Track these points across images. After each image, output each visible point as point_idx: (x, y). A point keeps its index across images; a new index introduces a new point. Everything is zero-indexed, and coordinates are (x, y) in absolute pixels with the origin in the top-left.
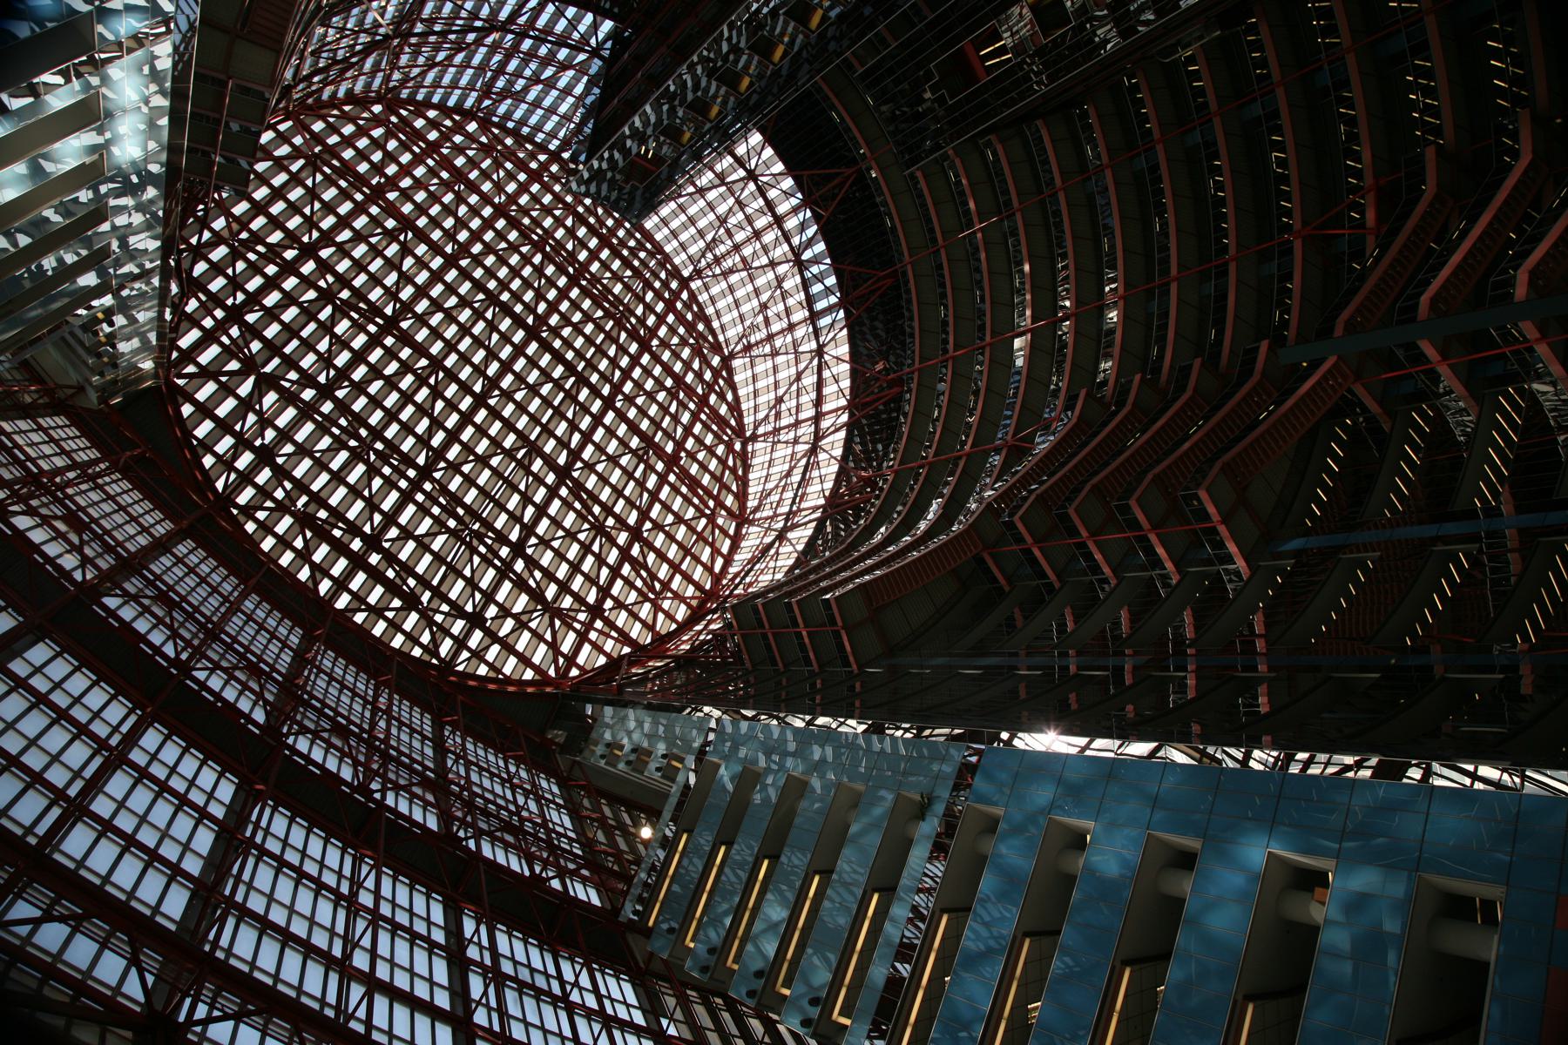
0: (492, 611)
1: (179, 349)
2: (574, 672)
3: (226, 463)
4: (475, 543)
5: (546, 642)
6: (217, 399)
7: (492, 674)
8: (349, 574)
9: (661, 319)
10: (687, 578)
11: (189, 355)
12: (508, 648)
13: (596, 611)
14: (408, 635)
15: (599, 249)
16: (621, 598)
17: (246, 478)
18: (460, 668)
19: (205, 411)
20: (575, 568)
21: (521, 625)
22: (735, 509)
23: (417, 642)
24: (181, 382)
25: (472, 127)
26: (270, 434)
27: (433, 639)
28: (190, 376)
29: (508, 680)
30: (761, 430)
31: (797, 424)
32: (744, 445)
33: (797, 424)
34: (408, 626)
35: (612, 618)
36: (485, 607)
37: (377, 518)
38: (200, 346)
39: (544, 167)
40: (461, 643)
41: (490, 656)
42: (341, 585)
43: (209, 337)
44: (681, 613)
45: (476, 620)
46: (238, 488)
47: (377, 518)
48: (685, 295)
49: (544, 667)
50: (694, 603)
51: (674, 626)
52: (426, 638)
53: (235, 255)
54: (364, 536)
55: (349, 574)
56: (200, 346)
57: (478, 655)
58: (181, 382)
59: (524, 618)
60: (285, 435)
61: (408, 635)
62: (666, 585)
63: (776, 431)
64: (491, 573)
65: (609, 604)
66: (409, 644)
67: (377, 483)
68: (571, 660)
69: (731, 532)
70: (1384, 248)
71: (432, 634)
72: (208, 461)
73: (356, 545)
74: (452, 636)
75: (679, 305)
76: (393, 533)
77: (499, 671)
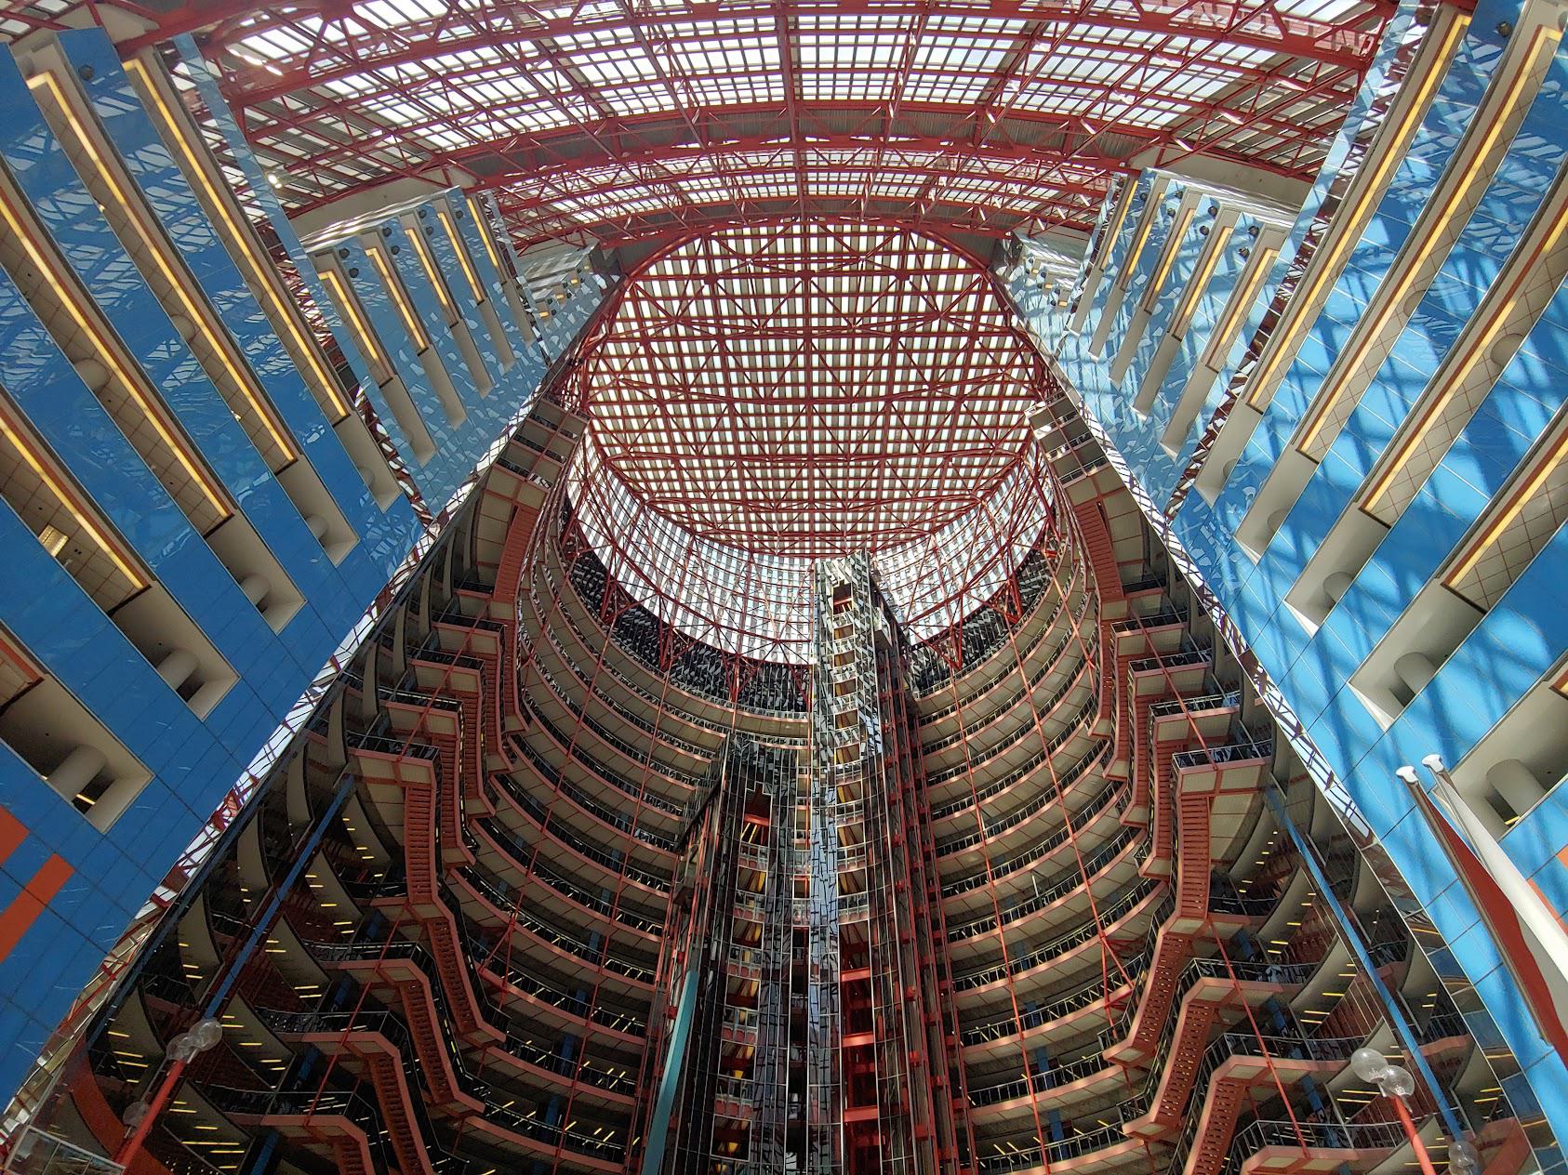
0: (706, 291)
1: (989, 293)
4: (748, 323)
5: (659, 298)
6: (950, 283)
7: (675, 253)
9: (748, 522)
10: (608, 403)
11: (981, 294)
12: (678, 277)
13: (645, 341)
15: (812, 527)
18: (697, 242)
19: (952, 271)
20: (679, 355)
21: (683, 297)
22: (616, 463)
23: (735, 237)
24: (976, 276)
25: (927, 527)
26: (908, 287)
27: (726, 247)
28: (973, 285)
29: (662, 258)
30: (642, 516)
31: (629, 540)
32: (643, 501)
33: (629, 540)
34: (748, 243)
36: (712, 290)
37: (814, 290)
38: (980, 303)
39: (874, 541)
40: (709, 257)
43: (978, 311)
45: (711, 278)
47: (814, 290)
48: (746, 544)
52: (732, 244)
53: (996, 365)
54: (813, 274)
56: (980, 303)
58: (976, 276)
60: (900, 294)
62: (618, 389)
63: (634, 525)
64: (725, 312)
65: (642, 351)
67: (830, 309)
68: (636, 300)
69: (606, 449)
70: (472, 973)
71: (731, 250)
72: (931, 245)
74: (717, 257)
75: (744, 537)
77: (673, 259)
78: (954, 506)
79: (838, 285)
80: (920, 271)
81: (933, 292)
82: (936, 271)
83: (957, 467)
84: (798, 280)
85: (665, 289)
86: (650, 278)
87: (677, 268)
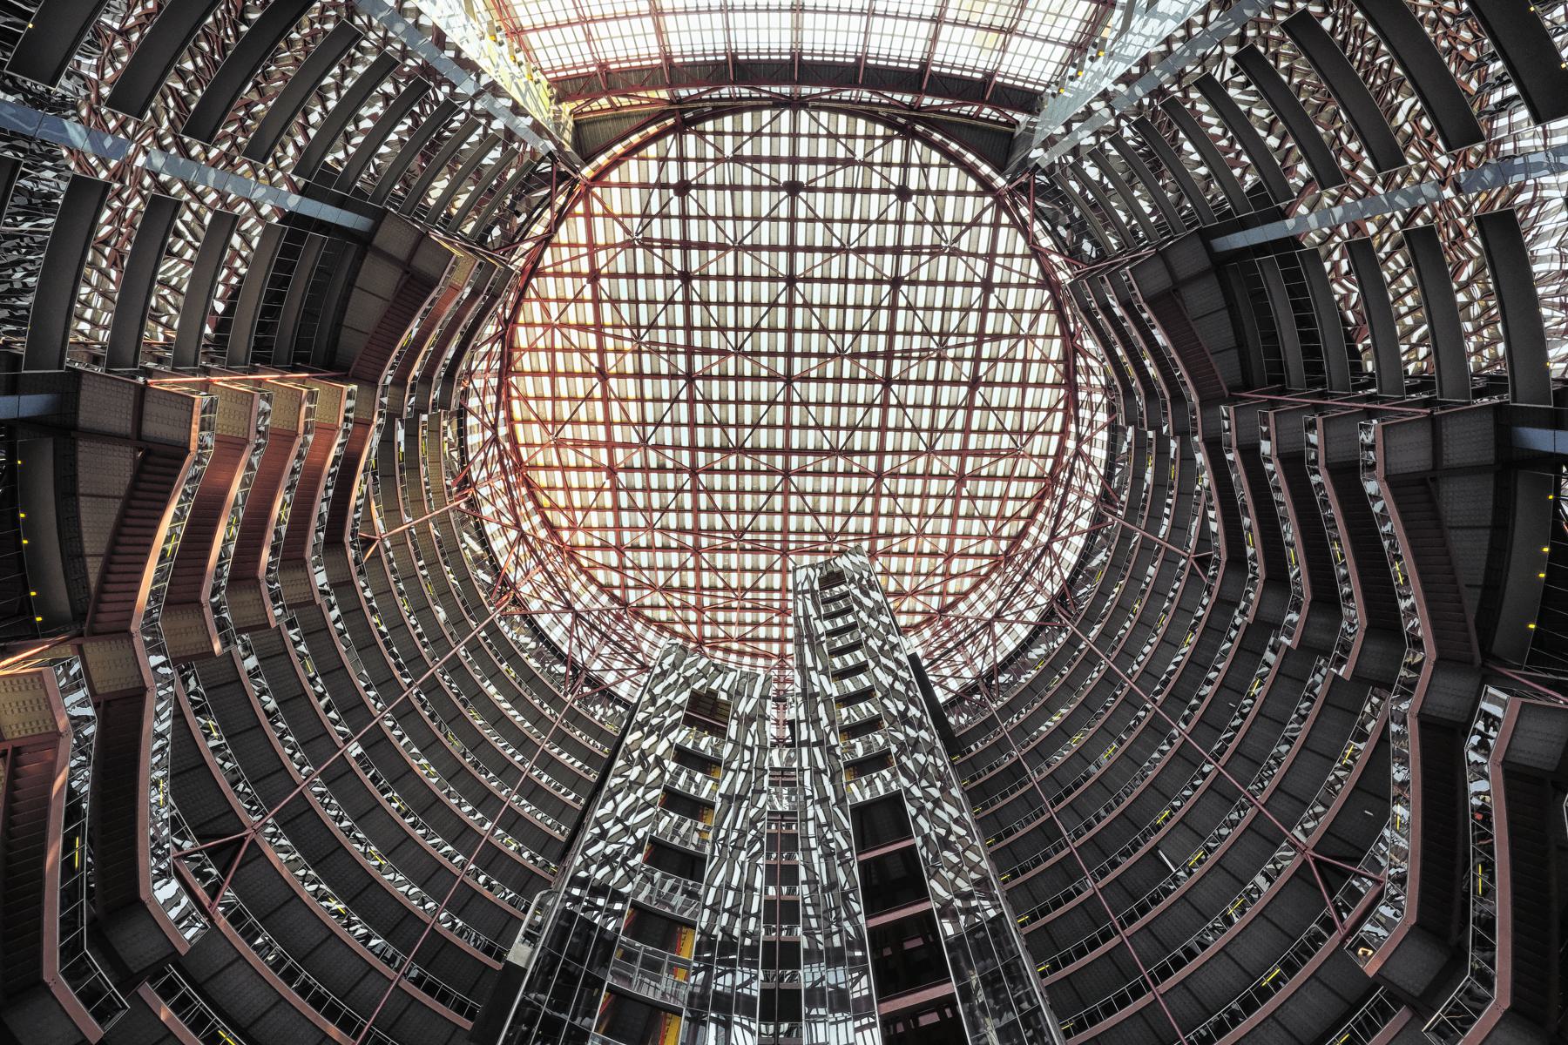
0: (674, 208)
3: (924, 166)
7: (642, 153)
8: (794, 147)
11: (996, 225)
14: (722, 133)
16: (580, 305)
17: (905, 165)
19: (961, 193)
23: (715, 133)
24: (989, 200)
28: (984, 210)
35: (577, 280)
41: (653, 165)
42: (794, 135)
44: (522, 337)
45: (683, 188)
49: (606, 190)
50: (516, 354)
51: (521, 320)
55: (794, 147)
57: (663, 160)
59: (646, 221)
61: (722, 133)
66: (719, 128)
68: (589, 215)
69: (523, 450)
72: (936, 157)
75: (692, 616)
76: (784, 211)
78: (970, 564)
81: (938, 221)
83: (973, 498)
84: (783, 194)
86: (609, 185)
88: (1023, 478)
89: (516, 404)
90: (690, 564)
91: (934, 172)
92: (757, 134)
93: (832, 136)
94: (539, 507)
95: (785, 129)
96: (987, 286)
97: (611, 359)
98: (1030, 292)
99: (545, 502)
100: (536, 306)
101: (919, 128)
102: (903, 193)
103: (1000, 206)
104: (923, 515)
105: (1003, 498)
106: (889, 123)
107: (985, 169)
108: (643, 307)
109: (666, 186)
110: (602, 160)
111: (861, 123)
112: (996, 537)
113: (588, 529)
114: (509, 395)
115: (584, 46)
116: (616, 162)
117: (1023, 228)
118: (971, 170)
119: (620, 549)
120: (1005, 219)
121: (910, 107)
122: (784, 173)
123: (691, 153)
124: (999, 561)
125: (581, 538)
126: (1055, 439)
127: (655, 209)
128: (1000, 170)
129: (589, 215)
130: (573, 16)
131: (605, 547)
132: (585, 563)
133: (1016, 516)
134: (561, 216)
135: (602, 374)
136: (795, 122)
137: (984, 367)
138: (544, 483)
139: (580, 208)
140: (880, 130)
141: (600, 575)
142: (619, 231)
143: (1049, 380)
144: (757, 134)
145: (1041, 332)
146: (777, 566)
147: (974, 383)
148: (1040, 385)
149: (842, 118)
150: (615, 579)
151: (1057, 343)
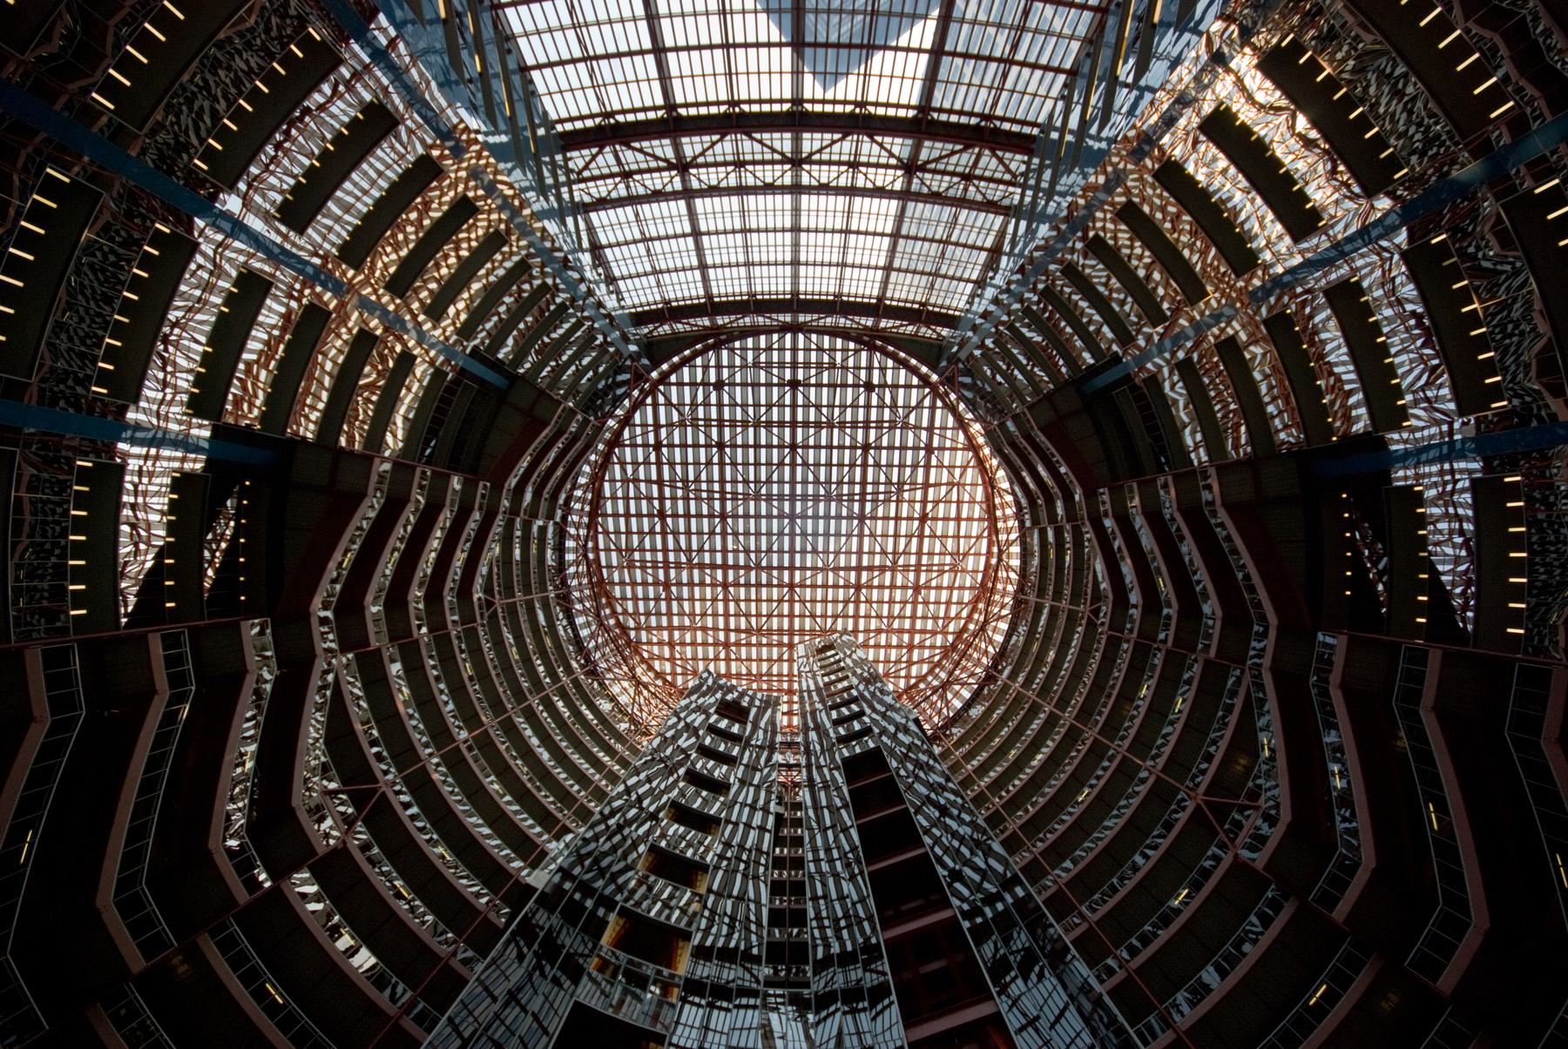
0: (713, 399)
2: (649, 400)
6: (907, 397)
11: (933, 408)
12: (693, 384)
17: (870, 368)
19: (908, 386)
40: (719, 367)
41: (699, 371)
42: (794, 350)
46: (870, 360)
68: (655, 405)
72: (890, 363)
73: (800, 375)
78: (927, 653)
79: (819, 396)
80: (883, 386)
82: (896, 386)
85: (681, 395)
86: (671, 384)
87: (693, 375)
88: (962, 588)
89: (601, 537)
90: (722, 656)
91: (889, 373)
92: (769, 349)
93: (820, 349)
94: (614, 613)
95: (788, 345)
96: (929, 449)
97: (668, 504)
98: (959, 453)
99: (619, 610)
100: (617, 467)
101: (879, 343)
102: (869, 387)
103: (935, 394)
104: (891, 617)
105: (948, 603)
106: (857, 340)
107: (924, 369)
108: (691, 468)
109: (709, 384)
110: (665, 367)
111: (839, 341)
112: (945, 633)
113: (649, 629)
114: (596, 532)
115: (655, 290)
116: (675, 368)
117: (953, 409)
118: (914, 371)
119: (671, 644)
120: (939, 403)
121: (871, 329)
122: (788, 375)
123: (725, 362)
124: (947, 651)
125: (644, 636)
126: (983, 559)
127: (700, 399)
128: (933, 368)
129: (655, 405)
130: (649, 269)
131: (661, 643)
132: (646, 655)
133: (958, 617)
134: (638, 405)
135: (662, 515)
136: (794, 341)
137: (930, 506)
138: (618, 595)
139: (649, 400)
140: (852, 345)
141: (657, 665)
142: (675, 414)
143: (976, 516)
144: (769, 349)
145: (969, 481)
146: (786, 657)
147: (923, 518)
148: (970, 519)
149: (826, 338)
150: (668, 667)
151: (980, 489)
